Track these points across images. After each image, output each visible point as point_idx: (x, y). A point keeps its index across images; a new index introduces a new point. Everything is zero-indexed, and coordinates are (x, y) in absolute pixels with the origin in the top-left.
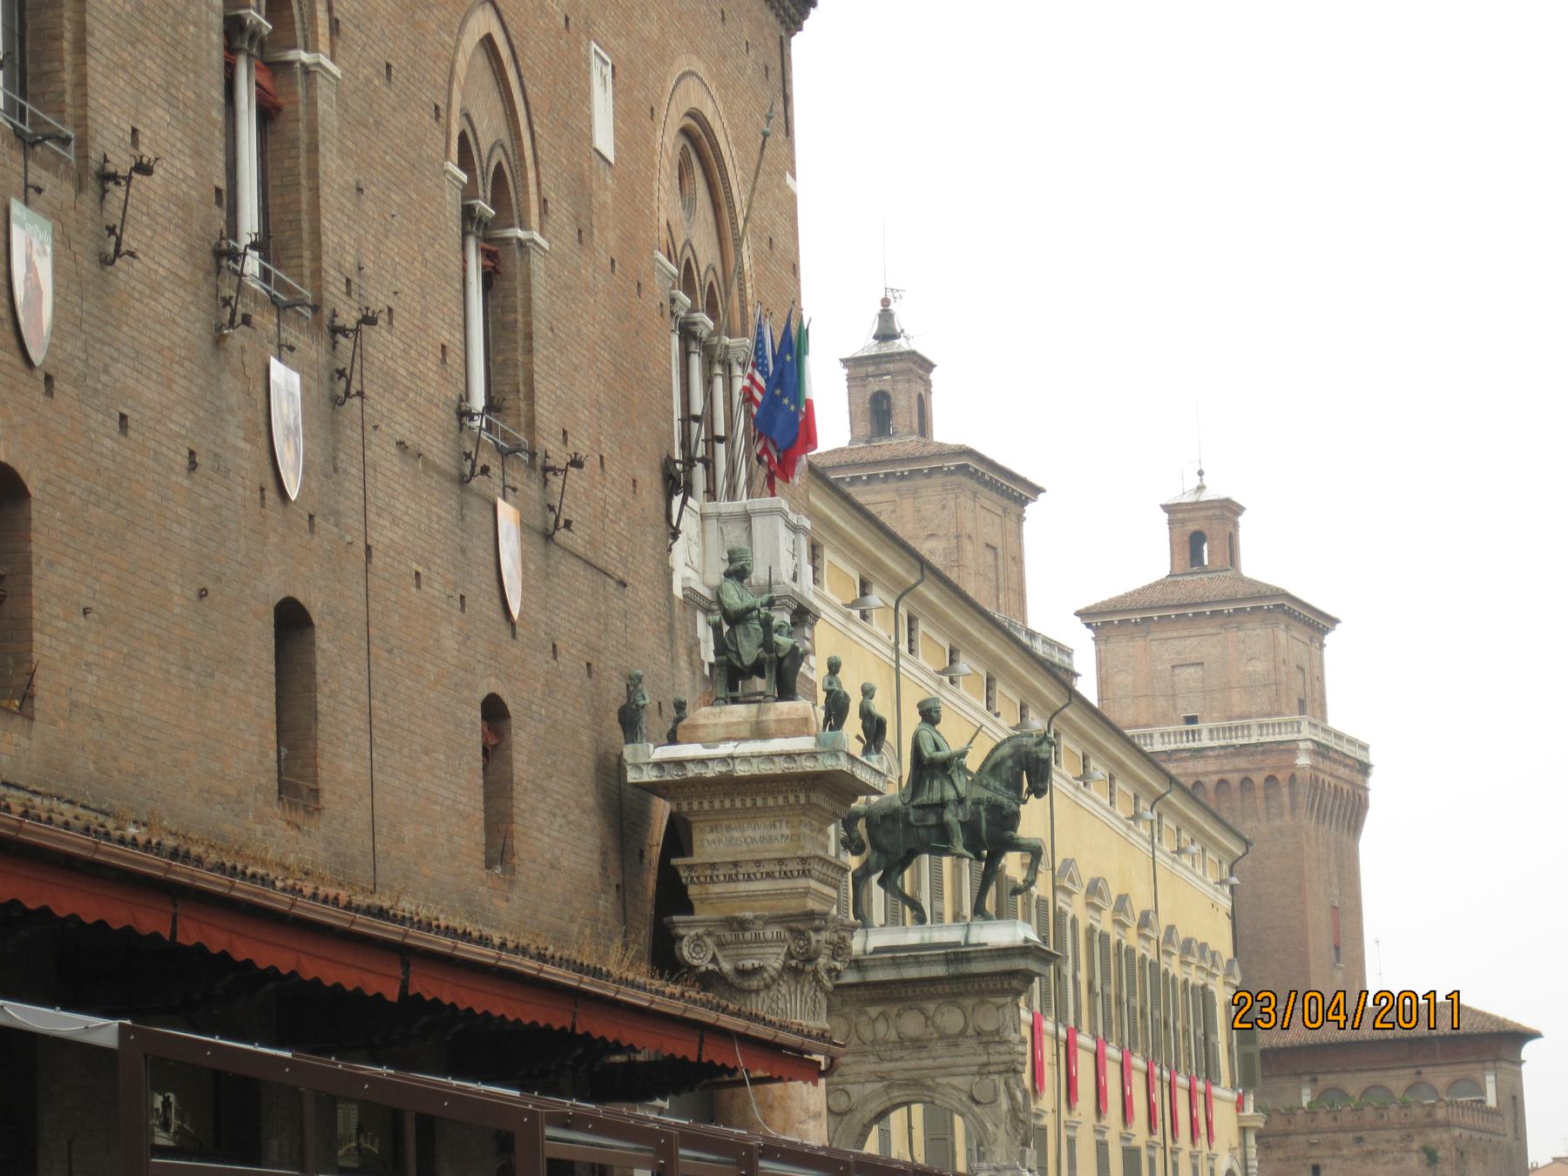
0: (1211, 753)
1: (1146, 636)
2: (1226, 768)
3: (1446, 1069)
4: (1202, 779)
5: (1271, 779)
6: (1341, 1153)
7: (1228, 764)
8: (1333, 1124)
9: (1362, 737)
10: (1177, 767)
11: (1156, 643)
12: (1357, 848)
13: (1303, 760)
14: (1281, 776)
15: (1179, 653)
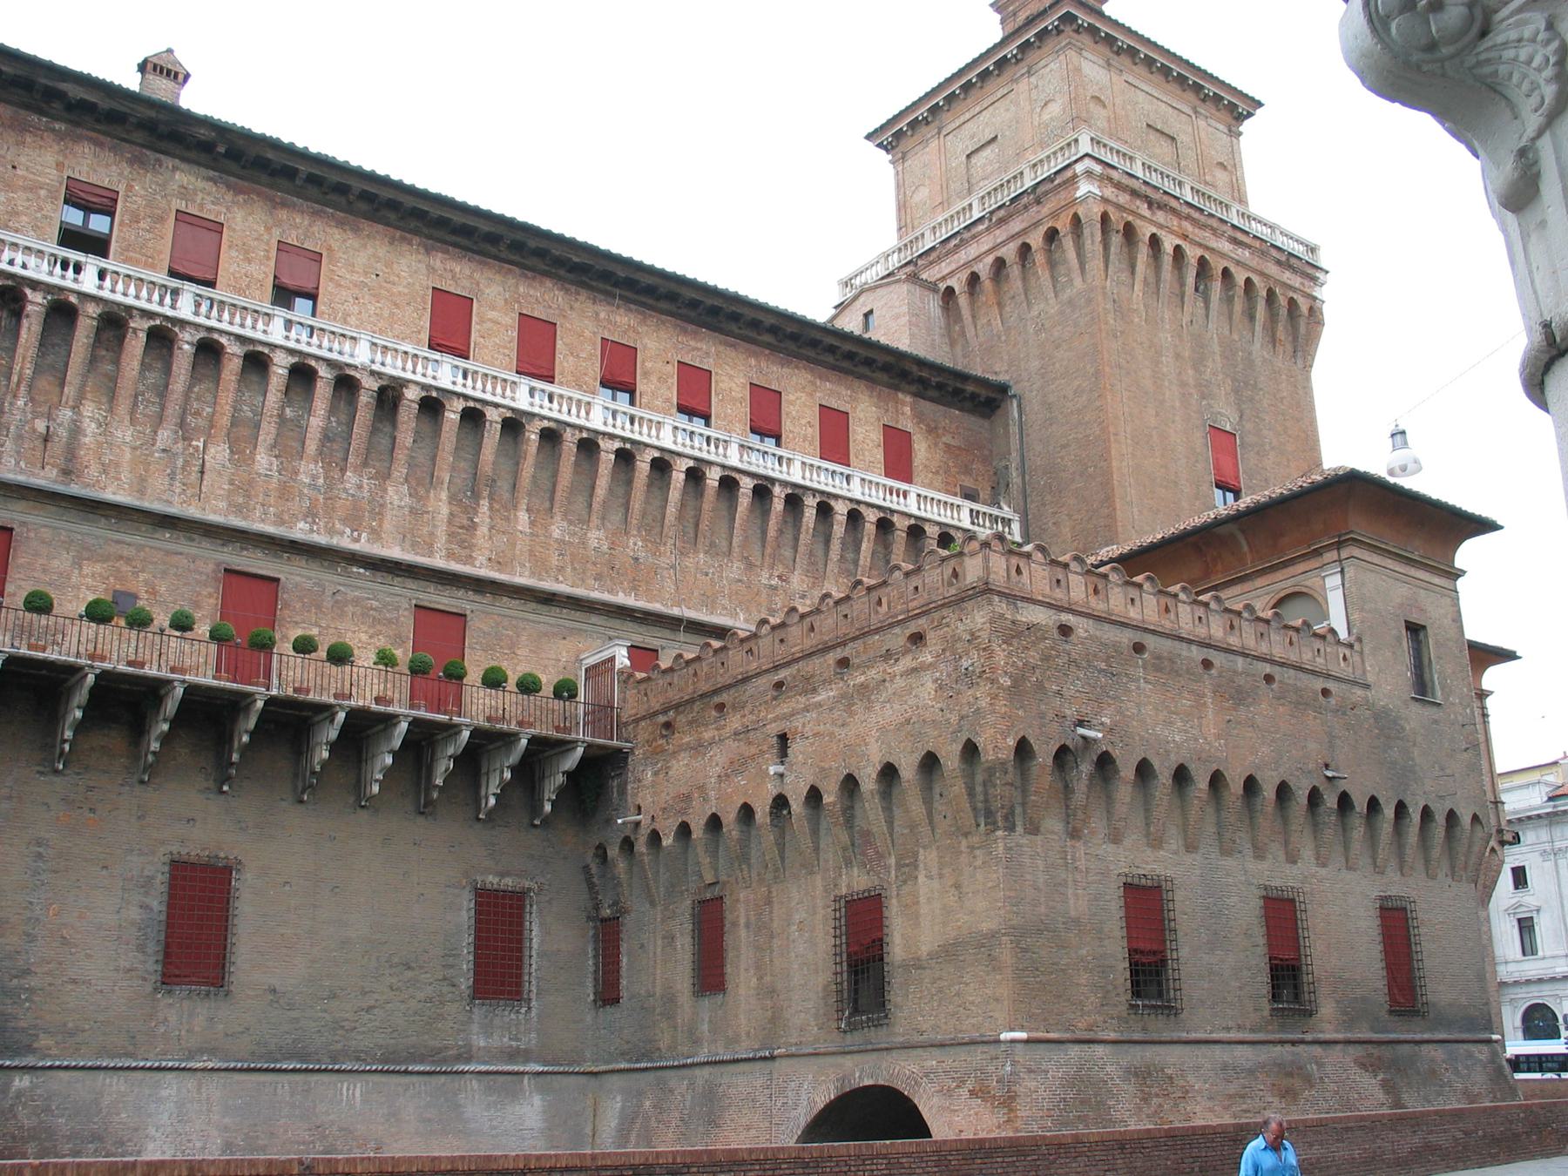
0: (981, 227)
1: (939, 133)
2: (999, 241)
3: (1259, 582)
4: (975, 269)
5: (1052, 235)
6: (818, 698)
7: (1000, 234)
8: (811, 642)
9: (1312, 239)
10: (949, 264)
11: (951, 136)
12: (1308, 379)
13: (1084, 188)
14: (1063, 225)
15: (972, 137)
